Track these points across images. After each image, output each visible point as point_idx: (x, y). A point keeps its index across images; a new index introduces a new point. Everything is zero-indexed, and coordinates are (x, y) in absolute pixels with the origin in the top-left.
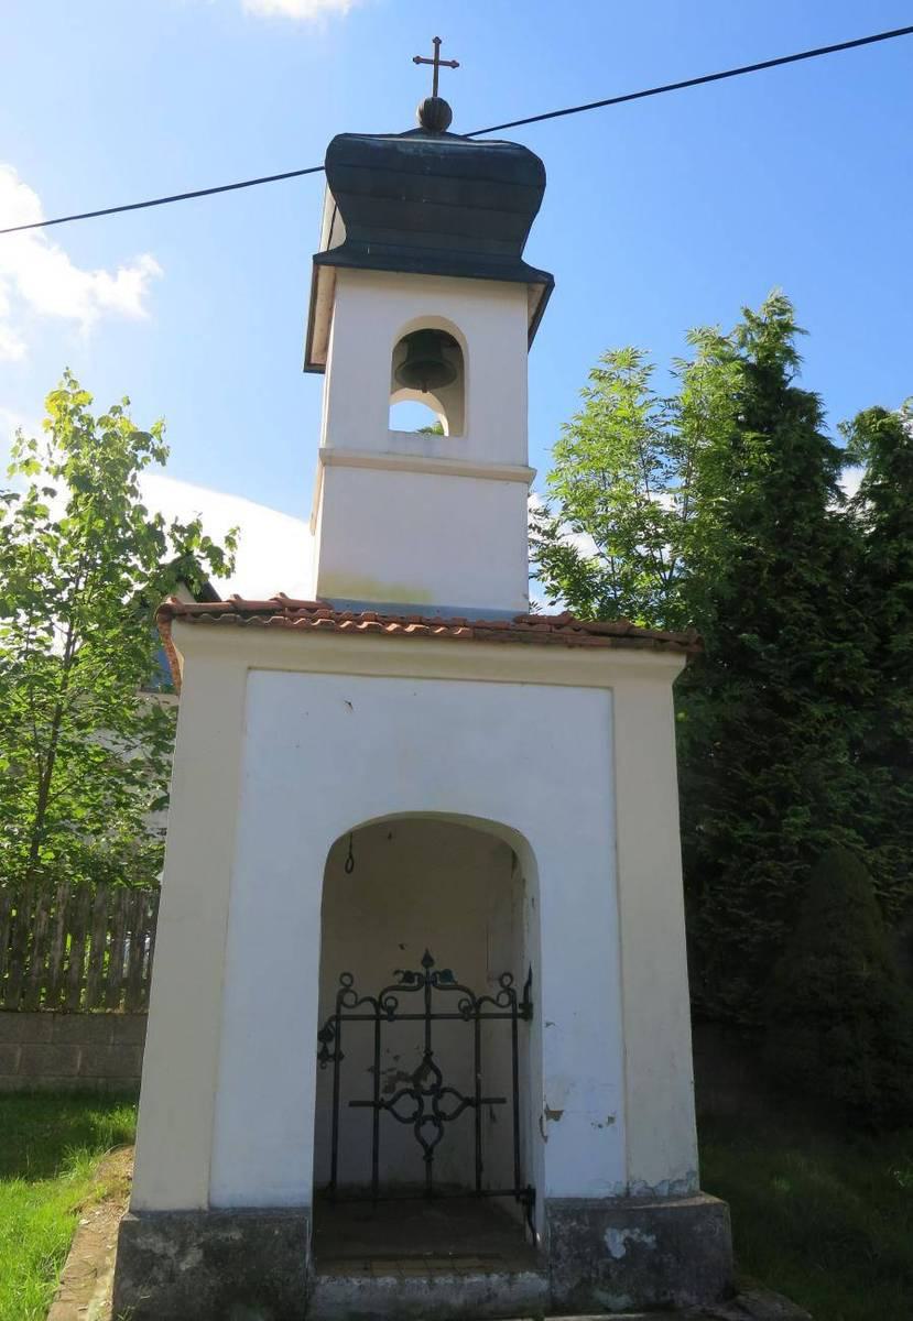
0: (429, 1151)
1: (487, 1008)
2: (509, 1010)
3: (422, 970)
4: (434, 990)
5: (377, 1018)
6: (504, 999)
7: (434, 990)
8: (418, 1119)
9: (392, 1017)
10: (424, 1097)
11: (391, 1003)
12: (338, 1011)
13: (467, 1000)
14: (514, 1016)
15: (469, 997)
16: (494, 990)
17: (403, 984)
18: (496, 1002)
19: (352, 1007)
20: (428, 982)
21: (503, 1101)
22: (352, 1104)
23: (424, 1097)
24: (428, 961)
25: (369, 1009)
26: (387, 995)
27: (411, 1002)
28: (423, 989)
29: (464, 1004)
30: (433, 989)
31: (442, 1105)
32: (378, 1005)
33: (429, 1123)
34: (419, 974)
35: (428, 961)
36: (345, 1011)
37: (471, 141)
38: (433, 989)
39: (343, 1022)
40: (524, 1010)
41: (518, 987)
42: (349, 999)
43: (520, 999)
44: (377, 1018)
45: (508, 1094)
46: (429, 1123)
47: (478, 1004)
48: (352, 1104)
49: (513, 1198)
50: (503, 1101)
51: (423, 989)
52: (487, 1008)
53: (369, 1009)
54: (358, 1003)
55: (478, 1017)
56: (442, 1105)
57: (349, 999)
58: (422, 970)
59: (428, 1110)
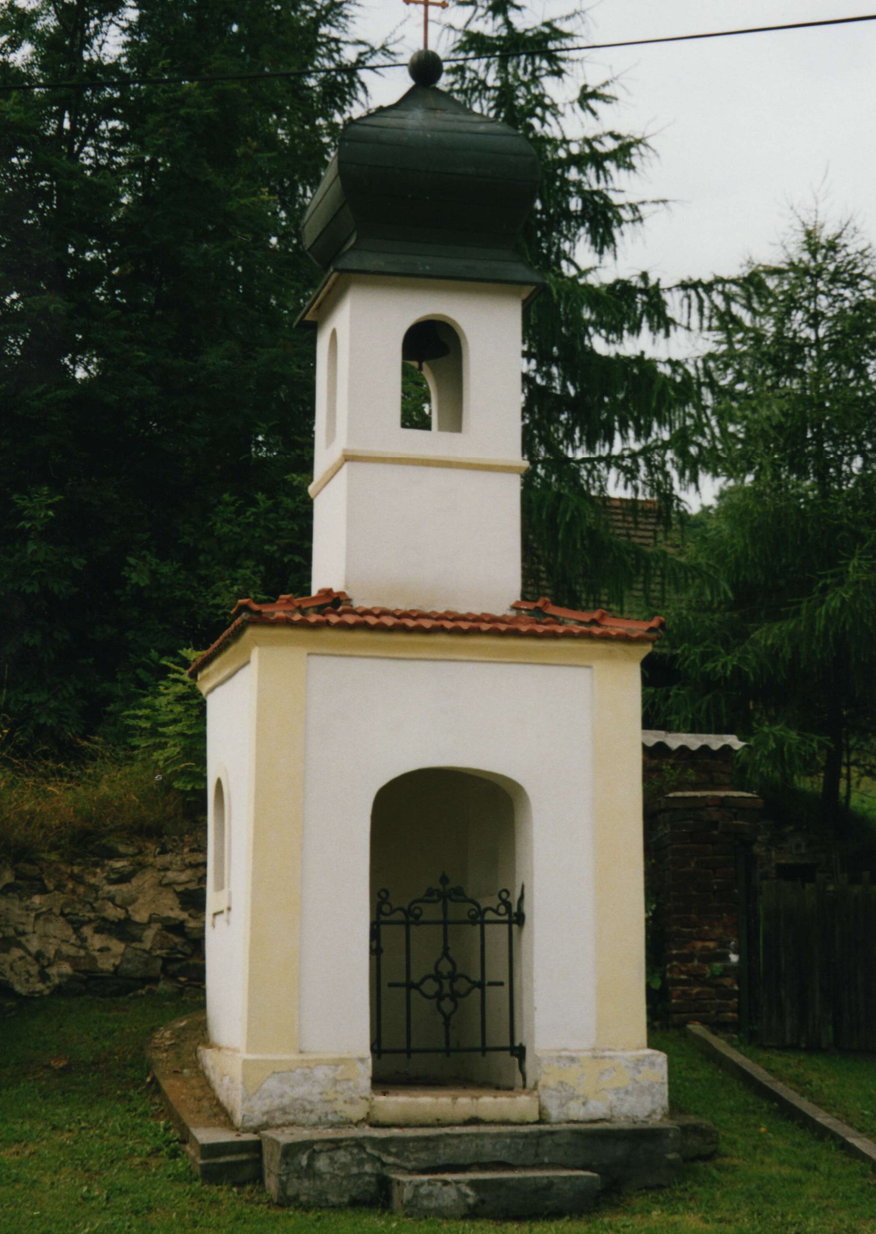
0: (447, 1018)
1: (490, 916)
2: (506, 918)
3: (441, 887)
4: (449, 903)
5: (407, 924)
6: (502, 909)
7: (449, 903)
8: (439, 996)
9: (418, 923)
10: (443, 981)
11: (417, 912)
12: (378, 917)
13: (474, 910)
14: (510, 923)
15: (475, 907)
16: (494, 902)
17: (427, 898)
18: (496, 912)
19: (389, 914)
20: (445, 897)
21: (501, 984)
22: (391, 985)
23: (443, 981)
24: (444, 880)
25: (399, 916)
26: (416, 905)
27: (432, 912)
28: (441, 903)
29: (473, 913)
30: (449, 901)
31: (456, 986)
32: (408, 913)
33: (447, 999)
34: (438, 890)
35: (444, 880)
36: (383, 918)
37: (365, 125)
38: (449, 901)
39: (382, 927)
40: (518, 919)
41: (514, 900)
42: (386, 908)
43: (515, 909)
44: (407, 924)
45: (505, 979)
46: (447, 999)
47: (482, 913)
48: (391, 985)
49: (508, 1053)
50: (501, 984)
51: (441, 903)
52: (490, 916)
53: (399, 916)
54: (393, 911)
55: (483, 923)
56: (456, 986)
57: (386, 908)
58: (441, 887)
59: (447, 989)
